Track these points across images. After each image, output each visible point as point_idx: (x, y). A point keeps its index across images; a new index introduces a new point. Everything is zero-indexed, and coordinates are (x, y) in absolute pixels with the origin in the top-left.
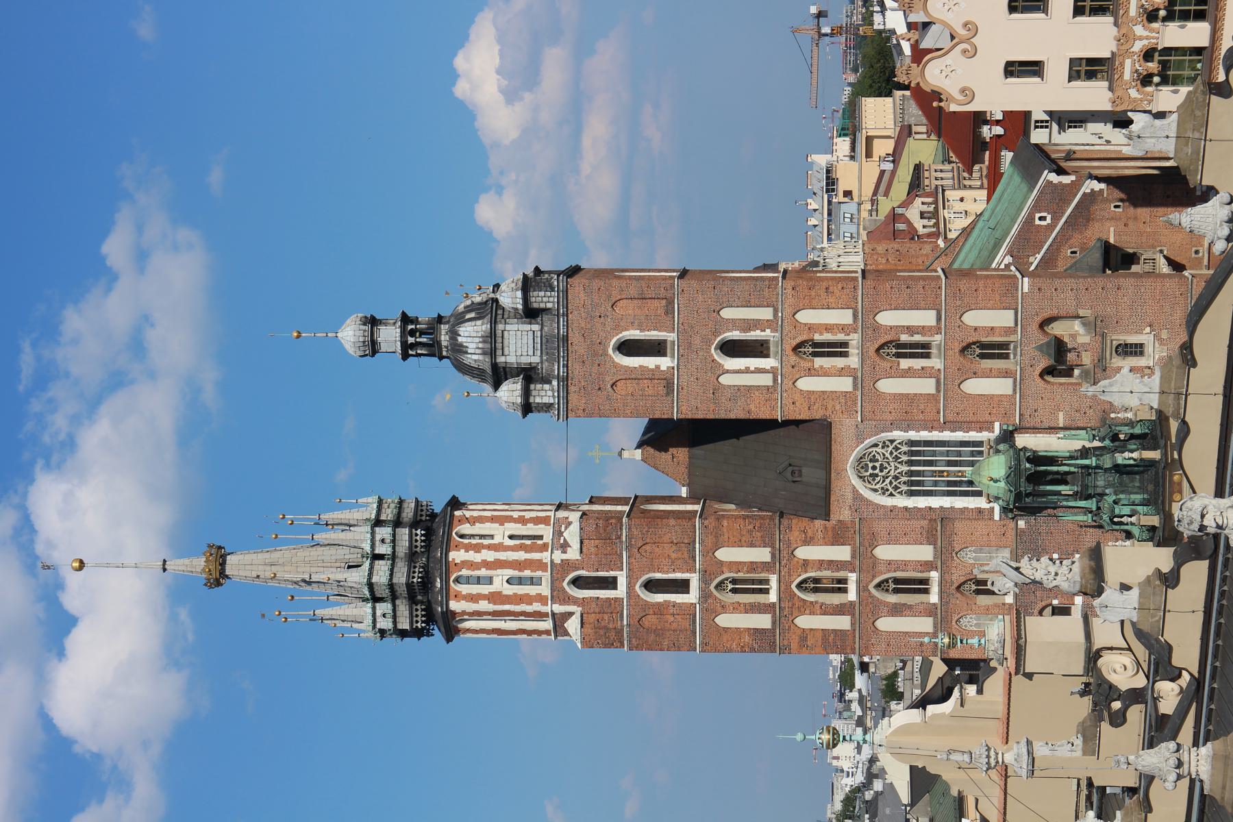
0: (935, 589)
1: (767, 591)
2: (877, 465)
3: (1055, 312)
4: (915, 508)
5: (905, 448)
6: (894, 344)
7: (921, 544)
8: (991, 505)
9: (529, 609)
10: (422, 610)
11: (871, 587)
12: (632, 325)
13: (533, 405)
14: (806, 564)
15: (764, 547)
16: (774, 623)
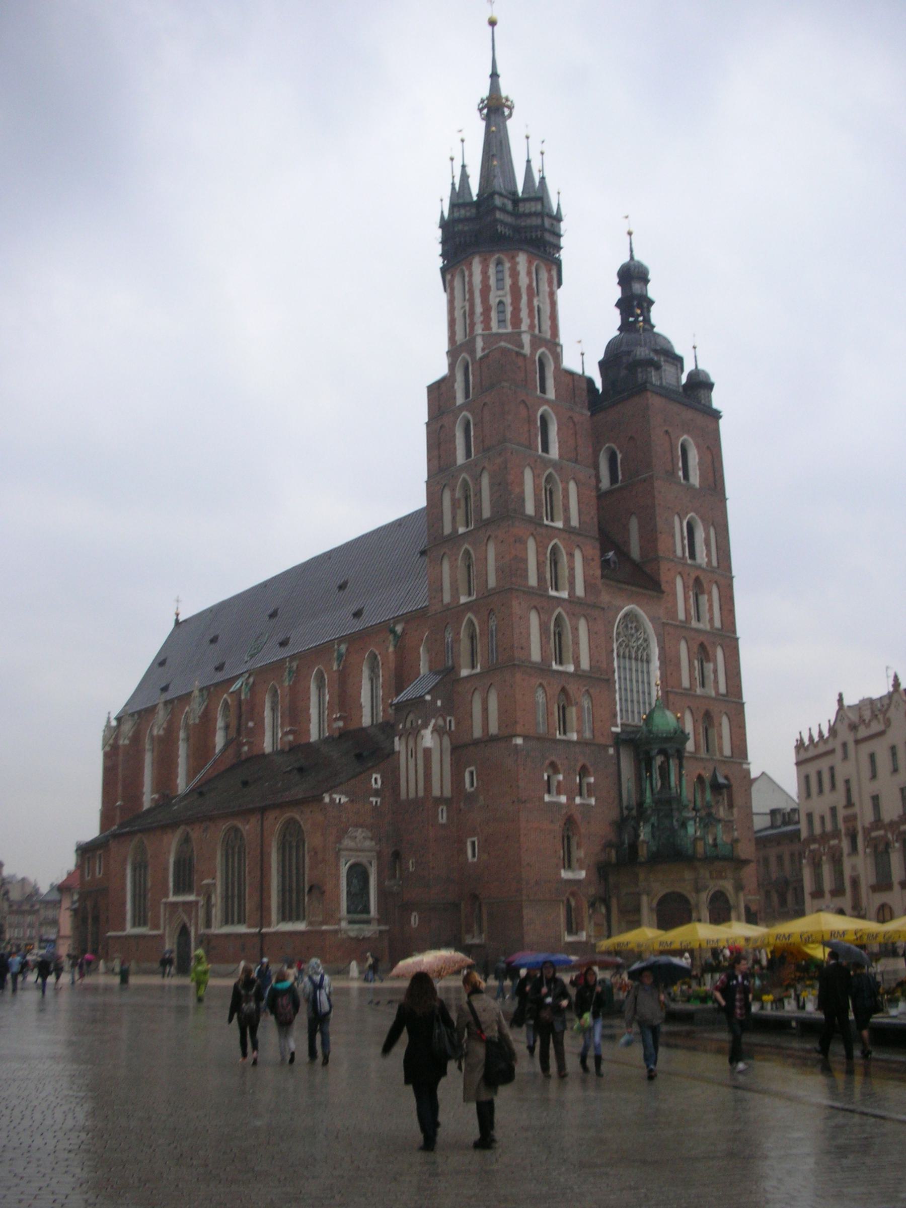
0: (560, 668)
1: (547, 519)
2: (633, 631)
3: (734, 788)
4: (614, 658)
5: (645, 657)
6: (703, 658)
7: (591, 661)
8: (619, 726)
9: (524, 314)
10: (509, 234)
11: (559, 610)
12: (700, 458)
13: (649, 369)
14: (571, 555)
15: (580, 524)
16: (530, 517)
